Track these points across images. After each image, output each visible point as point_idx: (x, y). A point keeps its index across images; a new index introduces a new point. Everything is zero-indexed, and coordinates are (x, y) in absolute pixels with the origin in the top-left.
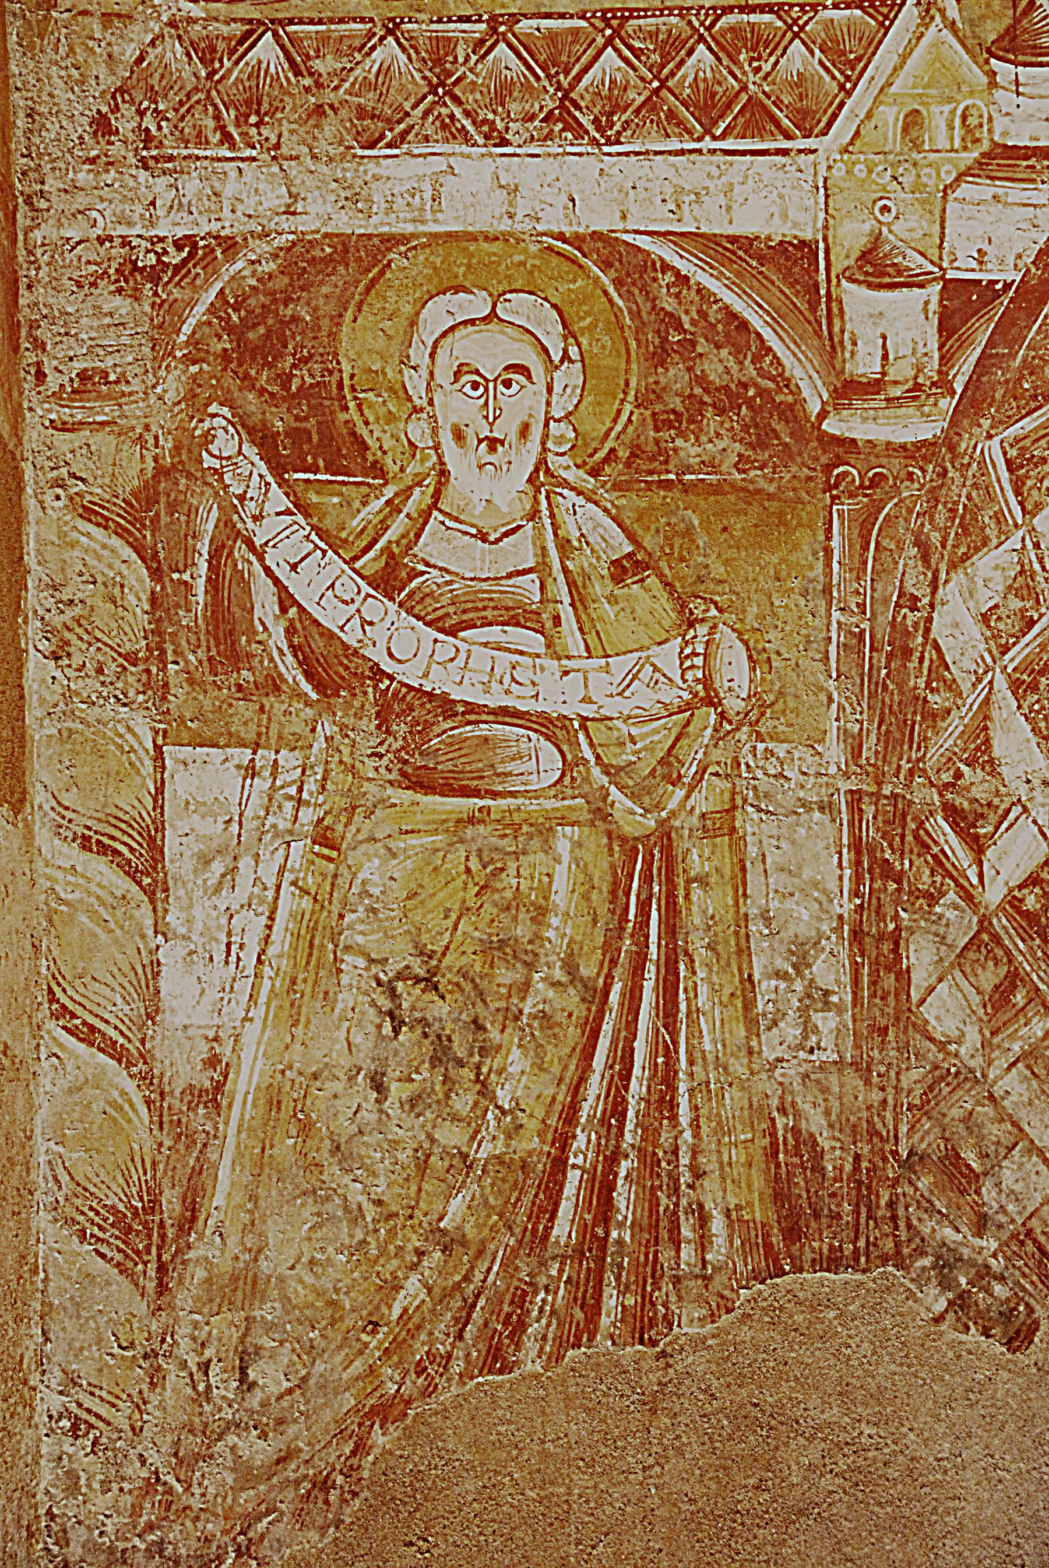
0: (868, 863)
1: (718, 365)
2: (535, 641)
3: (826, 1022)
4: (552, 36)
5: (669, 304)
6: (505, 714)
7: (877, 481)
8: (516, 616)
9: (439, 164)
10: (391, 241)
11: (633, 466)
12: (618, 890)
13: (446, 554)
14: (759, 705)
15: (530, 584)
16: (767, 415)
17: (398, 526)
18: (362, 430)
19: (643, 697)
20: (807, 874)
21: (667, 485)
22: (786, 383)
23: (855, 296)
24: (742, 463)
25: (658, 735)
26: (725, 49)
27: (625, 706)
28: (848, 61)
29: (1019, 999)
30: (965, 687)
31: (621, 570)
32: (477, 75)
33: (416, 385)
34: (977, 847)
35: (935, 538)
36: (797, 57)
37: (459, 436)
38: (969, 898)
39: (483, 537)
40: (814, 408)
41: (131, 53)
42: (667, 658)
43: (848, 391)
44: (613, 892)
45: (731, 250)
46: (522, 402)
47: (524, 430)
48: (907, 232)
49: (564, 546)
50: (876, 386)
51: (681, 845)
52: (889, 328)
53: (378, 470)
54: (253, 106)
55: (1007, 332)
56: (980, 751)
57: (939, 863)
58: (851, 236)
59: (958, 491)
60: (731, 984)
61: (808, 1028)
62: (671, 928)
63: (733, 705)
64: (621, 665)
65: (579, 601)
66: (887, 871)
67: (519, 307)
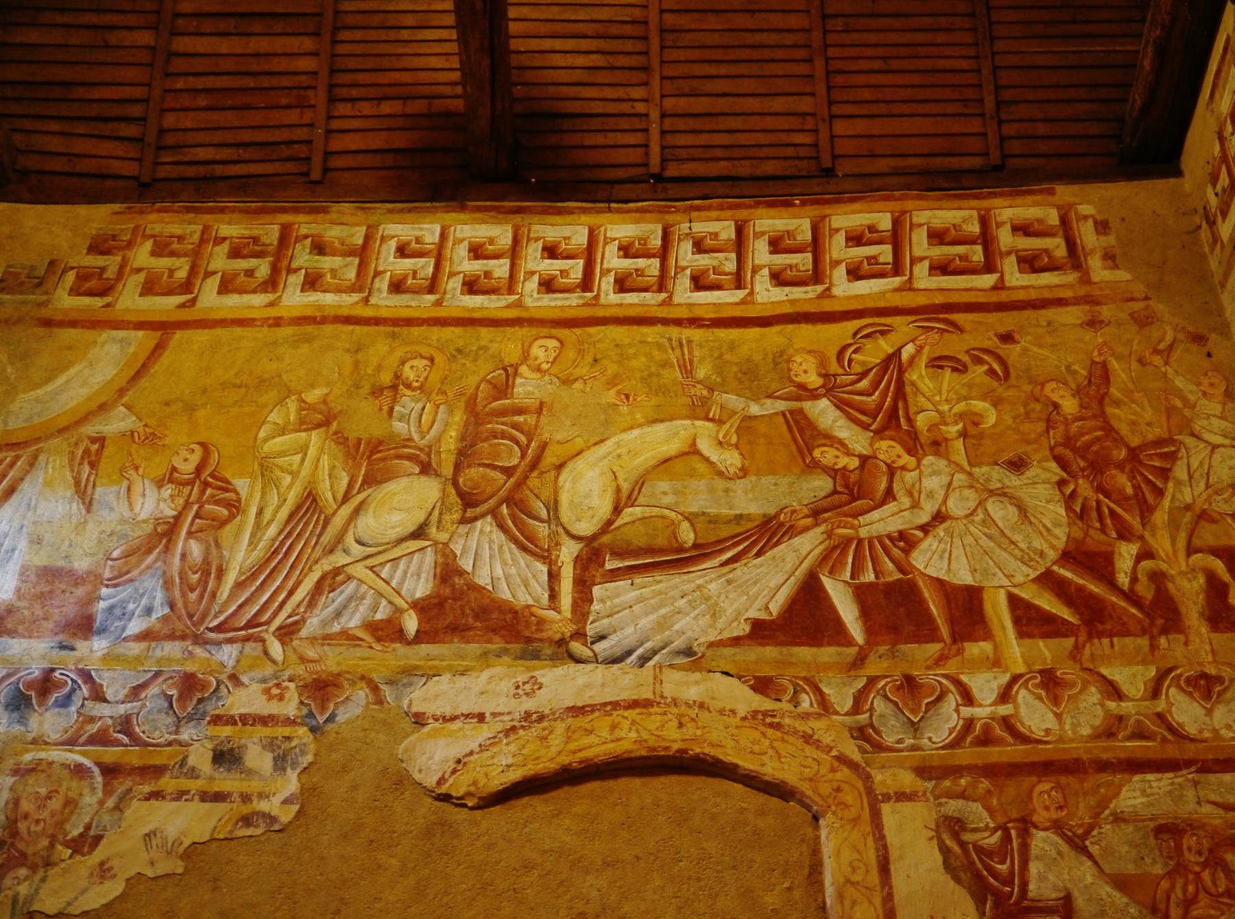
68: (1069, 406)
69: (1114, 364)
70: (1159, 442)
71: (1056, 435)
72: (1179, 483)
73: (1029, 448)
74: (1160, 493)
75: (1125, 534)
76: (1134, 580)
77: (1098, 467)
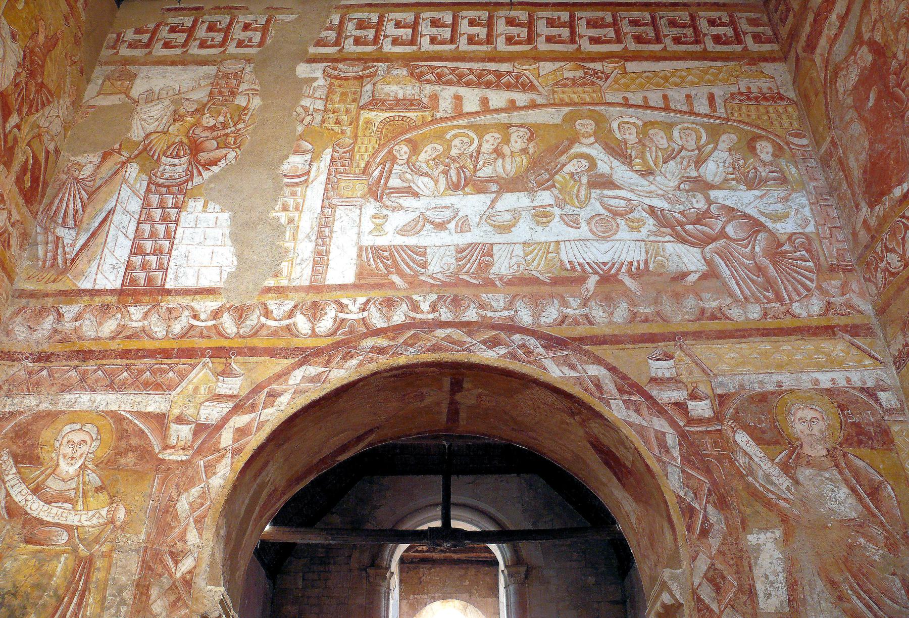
0: (146, 566)
1: (134, 441)
2: (69, 506)
3: (123, 609)
4: (112, 369)
5: (125, 427)
6: (57, 525)
7: (168, 470)
8: (66, 500)
9: (77, 396)
10: (60, 412)
11: (108, 464)
12: (74, 572)
13: (54, 485)
14: (125, 524)
15: (72, 493)
16: (144, 453)
17: (43, 477)
18: (40, 455)
19: (95, 521)
20: (128, 568)
21: (114, 469)
22: (151, 446)
23: (174, 427)
24: (135, 464)
25: (96, 531)
26: (153, 373)
27: (89, 523)
28: (182, 376)
29: (180, 604)
30: (182, 521)
31: (99, 489)
32: (92, 377)
33: (57, 444)
34: (176, 562)
35: (182, 483)
36: (171, 374)
37: (64, 456)
38: (171, 576)
39: (63, 480)
40: (157, 451)
41: (12, 372)
42: (104, 512)
43: (167, 448)
44: (73, 572)
45: (146, 416)
46: (84, 449)
47: (82, 455)
48: (190, 411)
49: (84, 483)
50: (173, 447)
51: (95, 559)
52: (182, 433)
53: (42, 464)
54: (37, 384)
55: (211, 435)
56: (183, 538)
57: (165, 566)
58: (176, 412)
59: (190, 472)
60: (98, 597)
61: (118, 610)
62: (86, 582)
63: (118, 523)
64: (90, 513)
65: (85, 495)
66: (150, 568)
67: (88, 427)
68: (41, 38)
69: (60, 43)
70: (49, 91)
71: (31, 44)
72: (43, 114)
73: (22, 36)
74: (37, 110)
75: (20, 111)
76: (10, 132)
77: (32, 74)
